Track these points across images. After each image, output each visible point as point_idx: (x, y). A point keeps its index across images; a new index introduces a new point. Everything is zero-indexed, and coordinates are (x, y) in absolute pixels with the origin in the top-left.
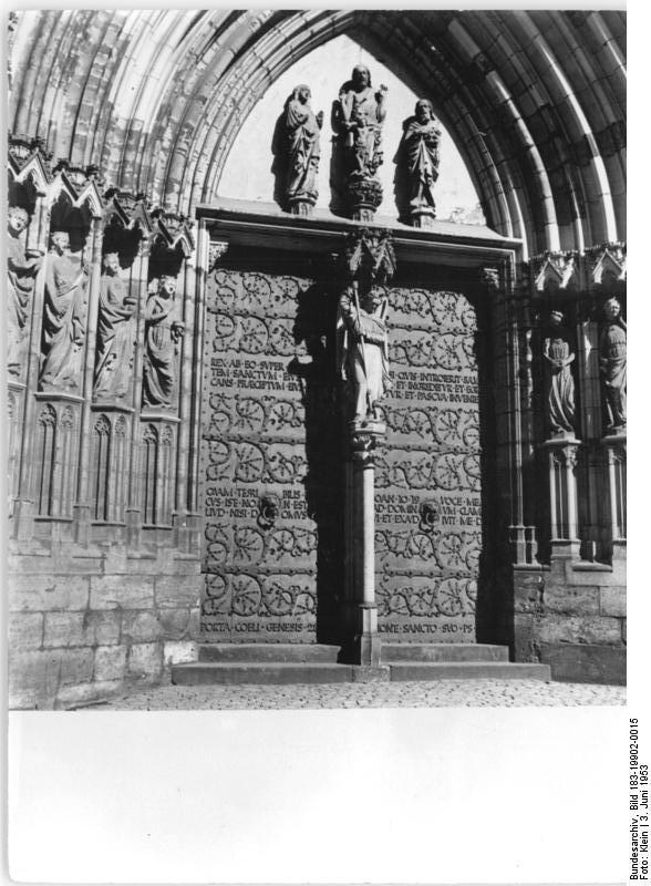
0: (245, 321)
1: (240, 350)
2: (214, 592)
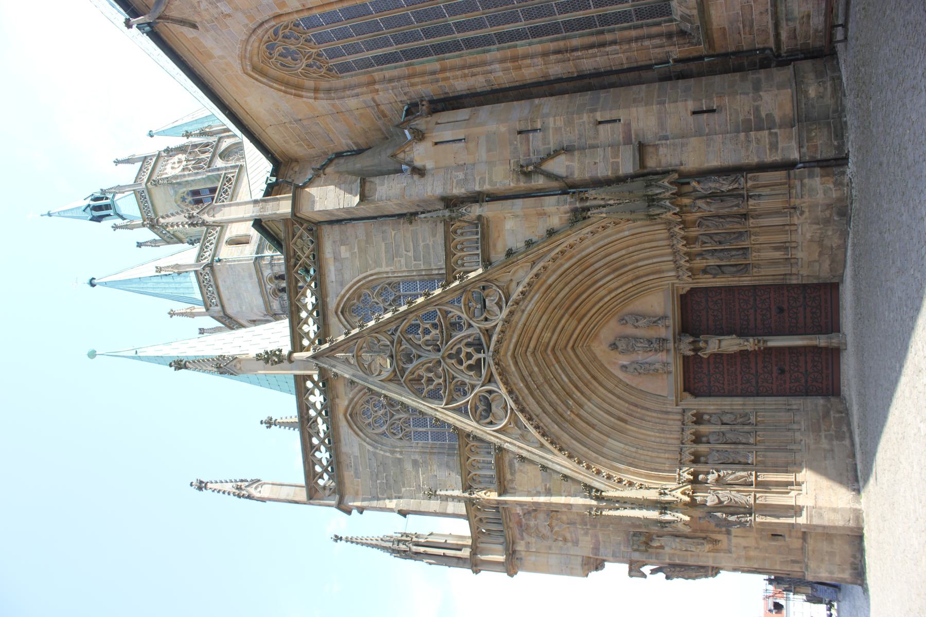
0: (712, 382)
1: (723, 384)
2: (815, 389)
